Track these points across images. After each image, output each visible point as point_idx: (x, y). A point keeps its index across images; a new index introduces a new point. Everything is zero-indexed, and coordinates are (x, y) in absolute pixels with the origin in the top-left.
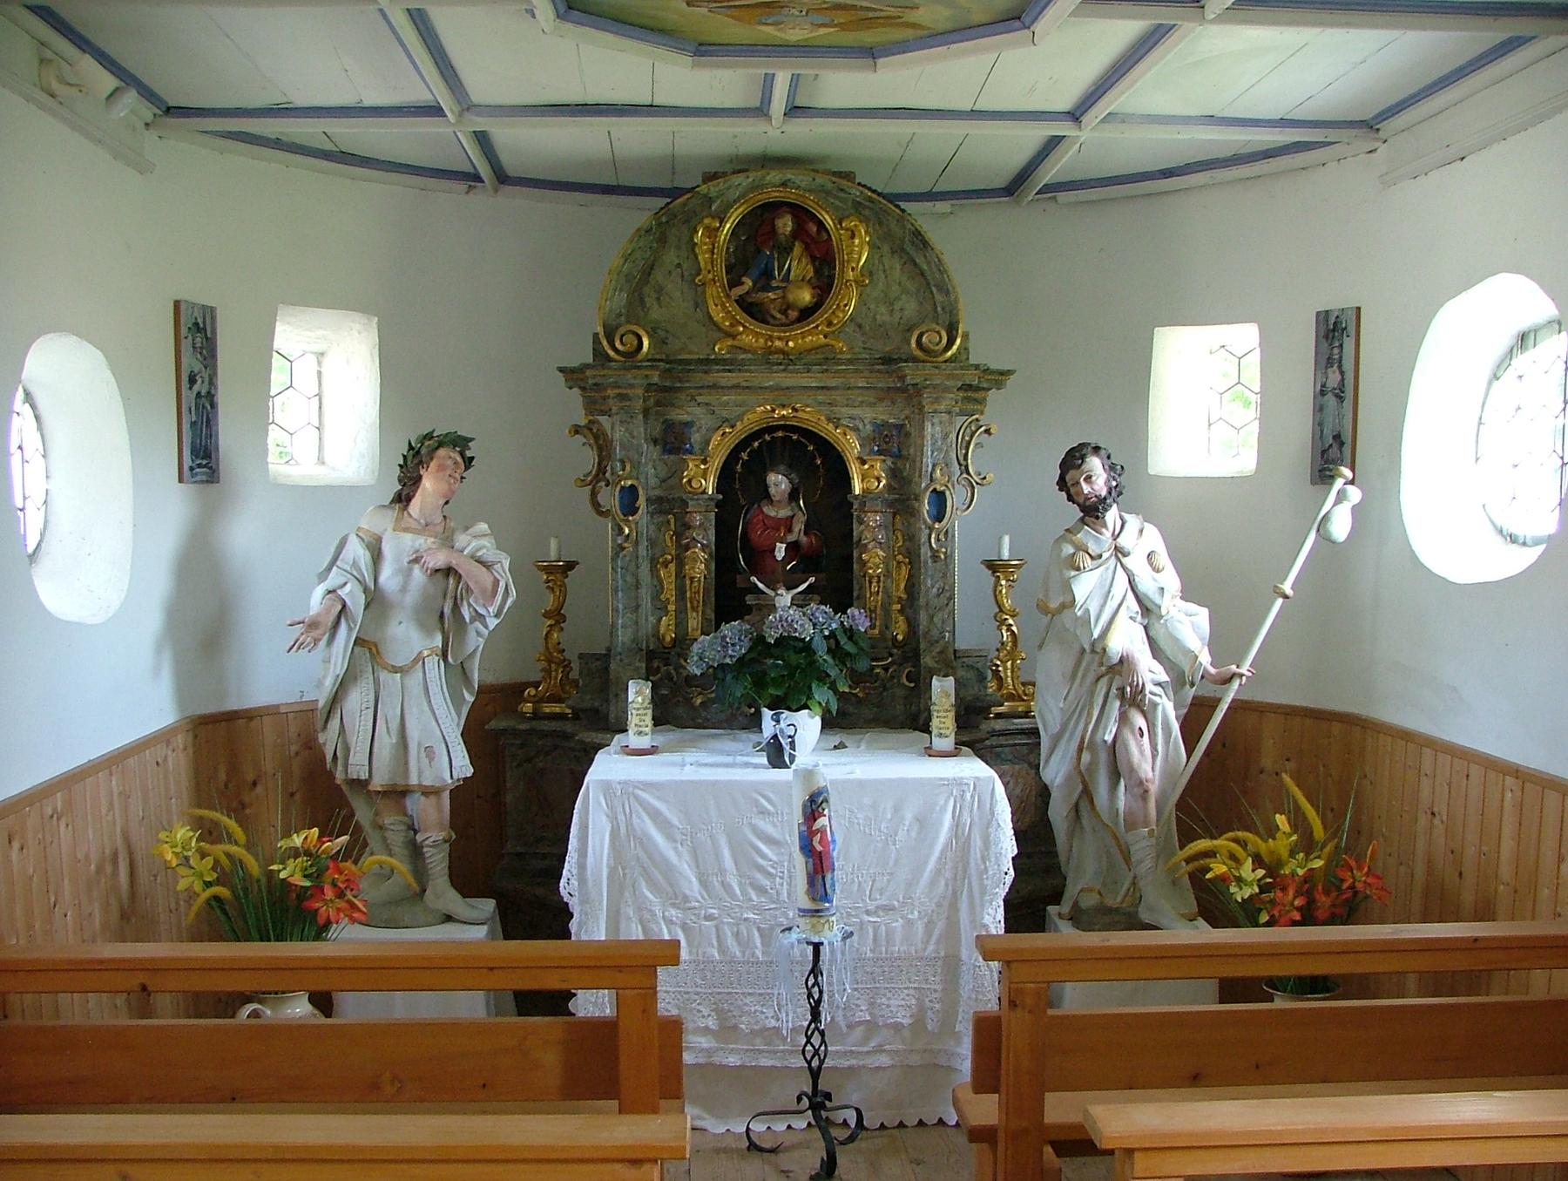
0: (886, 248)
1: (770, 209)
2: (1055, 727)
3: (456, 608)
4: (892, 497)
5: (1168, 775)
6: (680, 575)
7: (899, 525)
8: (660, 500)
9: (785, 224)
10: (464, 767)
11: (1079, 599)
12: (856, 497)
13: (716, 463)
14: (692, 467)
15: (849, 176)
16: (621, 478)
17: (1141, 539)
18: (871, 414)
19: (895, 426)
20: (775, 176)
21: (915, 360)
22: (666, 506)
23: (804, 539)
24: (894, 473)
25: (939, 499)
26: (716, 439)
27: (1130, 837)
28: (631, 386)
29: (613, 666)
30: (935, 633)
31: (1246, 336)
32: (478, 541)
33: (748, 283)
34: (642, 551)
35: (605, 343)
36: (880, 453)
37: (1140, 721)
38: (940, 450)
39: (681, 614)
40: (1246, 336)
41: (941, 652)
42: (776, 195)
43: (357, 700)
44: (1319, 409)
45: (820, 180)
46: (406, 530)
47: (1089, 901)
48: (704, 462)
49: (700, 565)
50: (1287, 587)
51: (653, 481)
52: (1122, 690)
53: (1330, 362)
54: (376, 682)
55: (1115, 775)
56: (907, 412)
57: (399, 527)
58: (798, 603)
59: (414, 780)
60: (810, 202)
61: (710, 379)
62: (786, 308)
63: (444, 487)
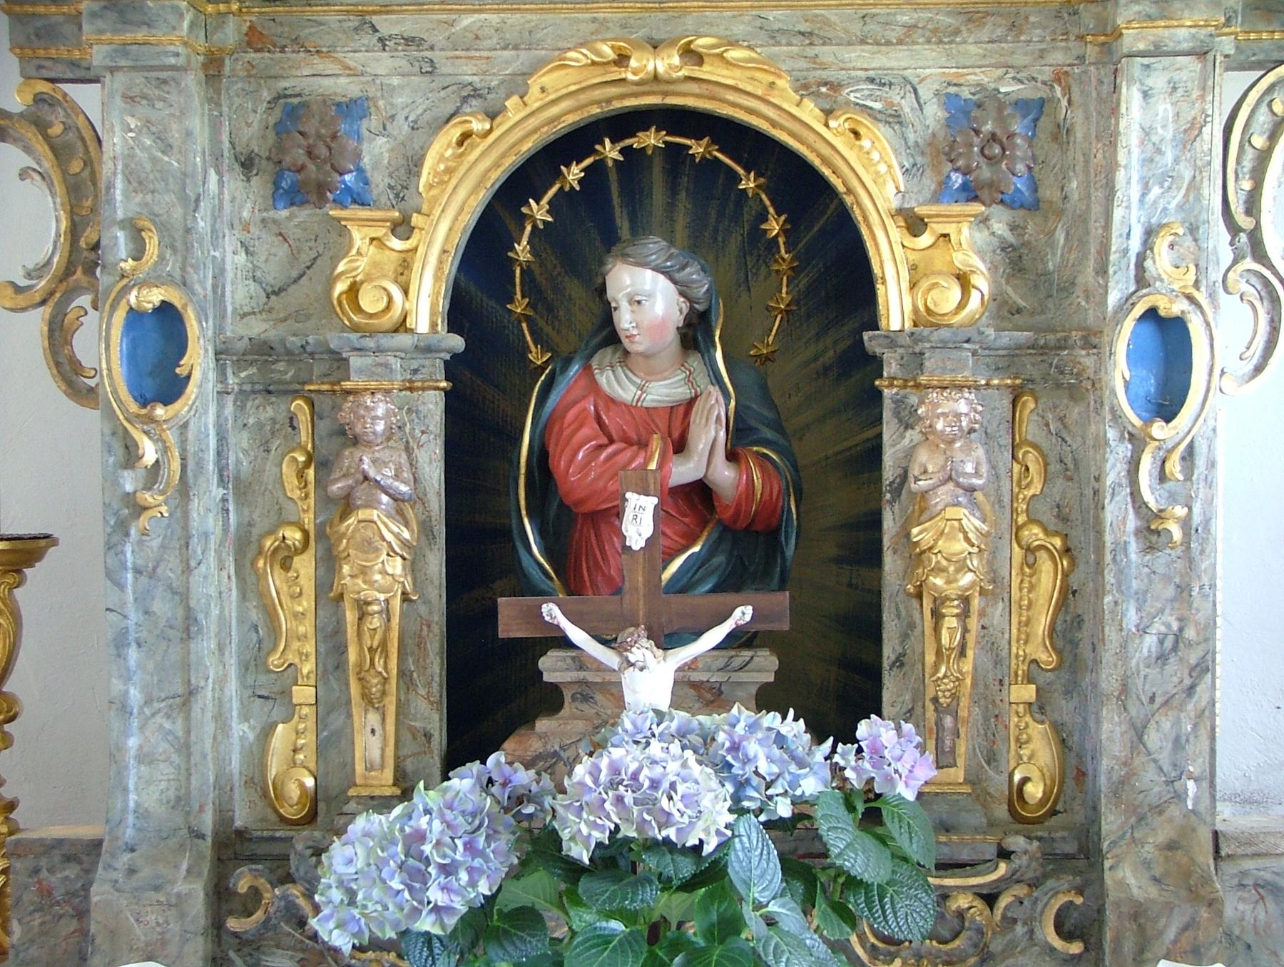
4: (1007, 338)
6: (329, 595)
7: (1030, 428)
8: (262, 351)
12: (892, 340)
14: (364, 248)
16: (129, 282)
19: (1022, 106)
22: (284, 371)
23: (725, 475)
24: (1015, 260)
26: (441, 148)
29: (99, 893)
30: (1150, 781)
34: (208, 510)
36: (970, 193)
38: (1169, 179)
39: (331, 710)
41: (1171, 846)
48: (402, 227)
49: (394, 562)
51: (239, 293)
56: (1058, 57)
58: (698, 692)
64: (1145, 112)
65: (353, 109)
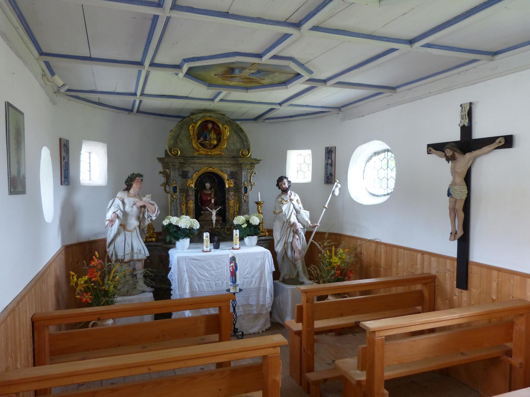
0: (233, 132)
1: (207, 122)
2: (279, 239)
3: (143, 215)
5: (303, 248)
8: (181, 189)
9: (210, 126)
10: (147, 254)
11: (284, 211)
13: (195, 181)
14: (189, 181)
15: (224, 115)
17: (296, 197)
18: (229, 170)
20: (208, 114)
21: (241, 157)
24: (235, 183)
25: (246, 189)
26: (194, 175)
27: (296, 263)
28: (176, 163)
31: (309, 152)
32: (147, 199)
33: (202, 139)
34: (178, 201)
35: (169, 152)
36: (232, 178)
37: (297, 237)
40: (309, 152)
42: (208, 119)
43: (120, 239)
44: (326, 168)
45: (218, 116)
46: (131, 197)
47: (287, 277)
50: (326, 206)
51: (180, 185)
52: (293, 230)
53: (329, 158)
54: (125, 235)
55: (292, 248)
57: (128, 196)
59: (135, 258)
60: (215, 120)
61: (193, 161)
62: (211, 145)
63: (139, 186)
64: (244, 173)
65: (188, 172)
